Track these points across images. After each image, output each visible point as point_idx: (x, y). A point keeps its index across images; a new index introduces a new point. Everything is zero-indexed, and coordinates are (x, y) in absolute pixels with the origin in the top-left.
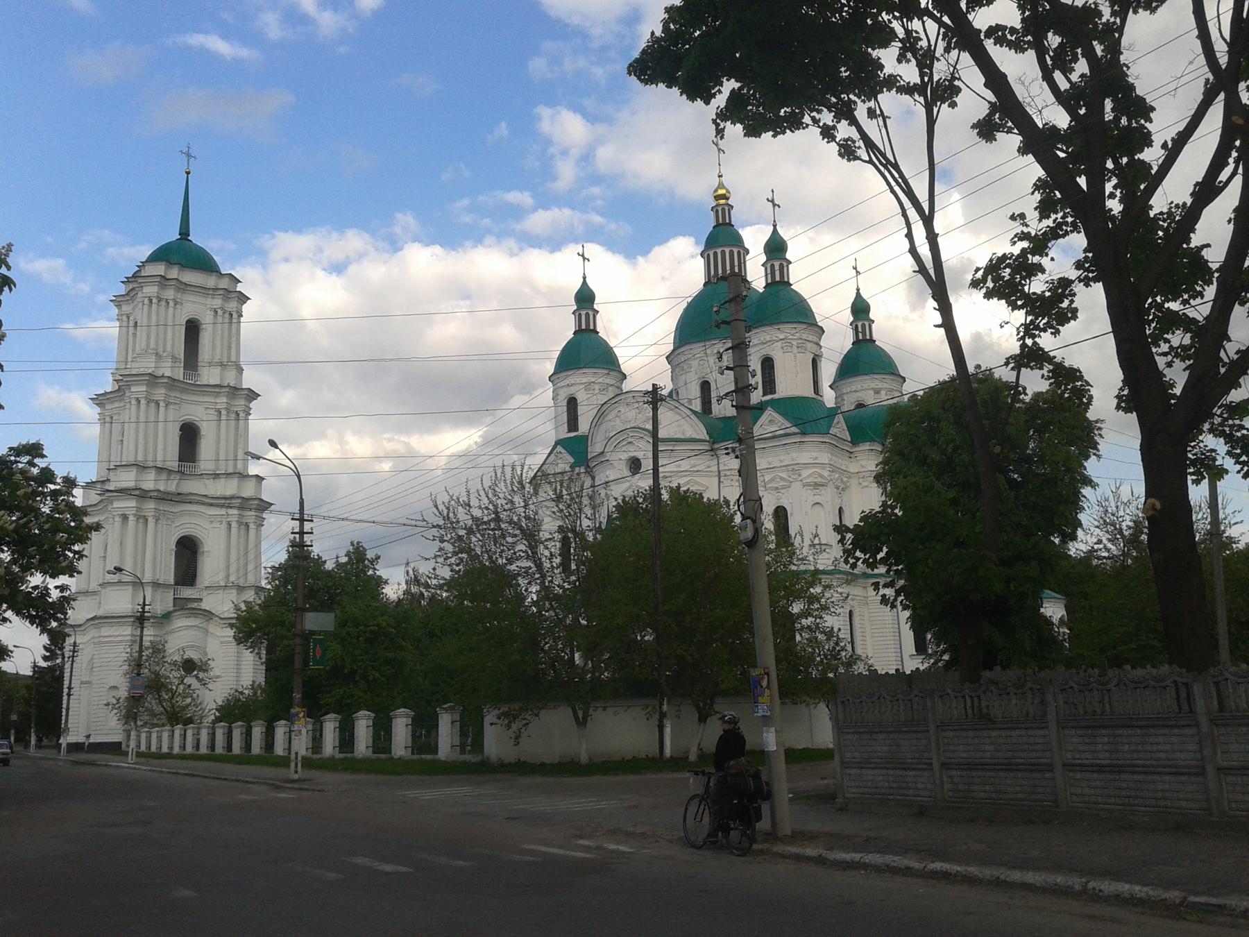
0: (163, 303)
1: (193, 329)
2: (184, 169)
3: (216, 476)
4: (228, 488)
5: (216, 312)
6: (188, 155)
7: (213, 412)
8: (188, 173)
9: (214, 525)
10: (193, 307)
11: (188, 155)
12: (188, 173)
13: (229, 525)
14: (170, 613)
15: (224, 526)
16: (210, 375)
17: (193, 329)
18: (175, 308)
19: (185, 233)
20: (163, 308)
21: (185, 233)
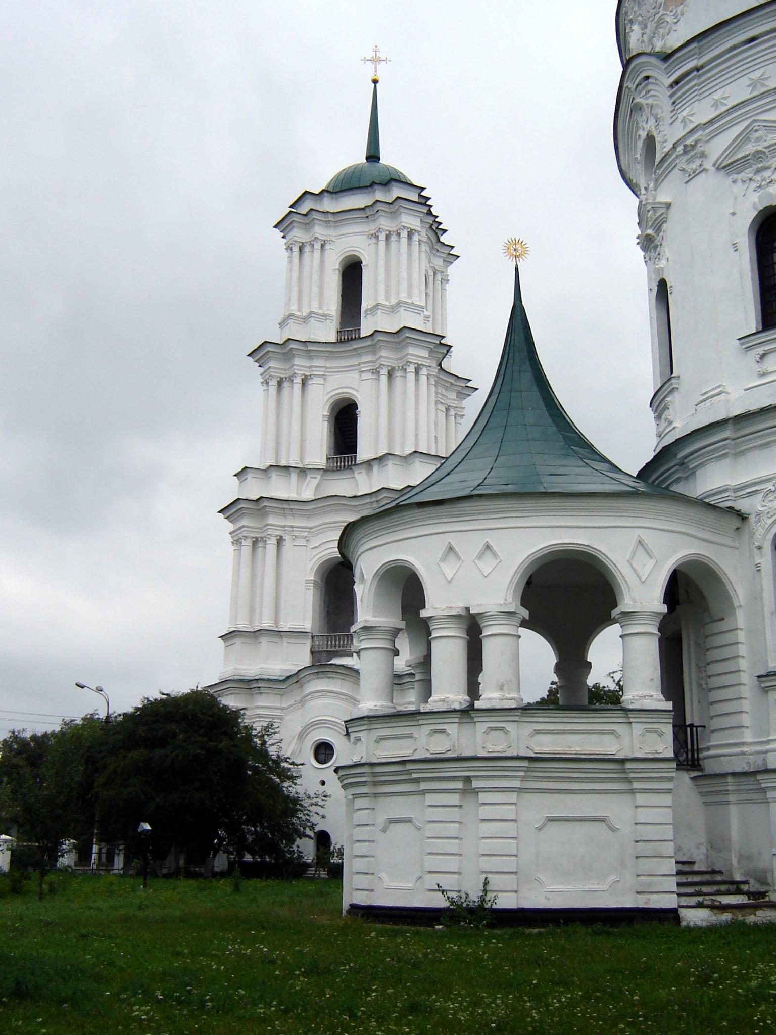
1: (352, 273)
8: (375, 82)
12: (375, 82)
17: (352, 273)
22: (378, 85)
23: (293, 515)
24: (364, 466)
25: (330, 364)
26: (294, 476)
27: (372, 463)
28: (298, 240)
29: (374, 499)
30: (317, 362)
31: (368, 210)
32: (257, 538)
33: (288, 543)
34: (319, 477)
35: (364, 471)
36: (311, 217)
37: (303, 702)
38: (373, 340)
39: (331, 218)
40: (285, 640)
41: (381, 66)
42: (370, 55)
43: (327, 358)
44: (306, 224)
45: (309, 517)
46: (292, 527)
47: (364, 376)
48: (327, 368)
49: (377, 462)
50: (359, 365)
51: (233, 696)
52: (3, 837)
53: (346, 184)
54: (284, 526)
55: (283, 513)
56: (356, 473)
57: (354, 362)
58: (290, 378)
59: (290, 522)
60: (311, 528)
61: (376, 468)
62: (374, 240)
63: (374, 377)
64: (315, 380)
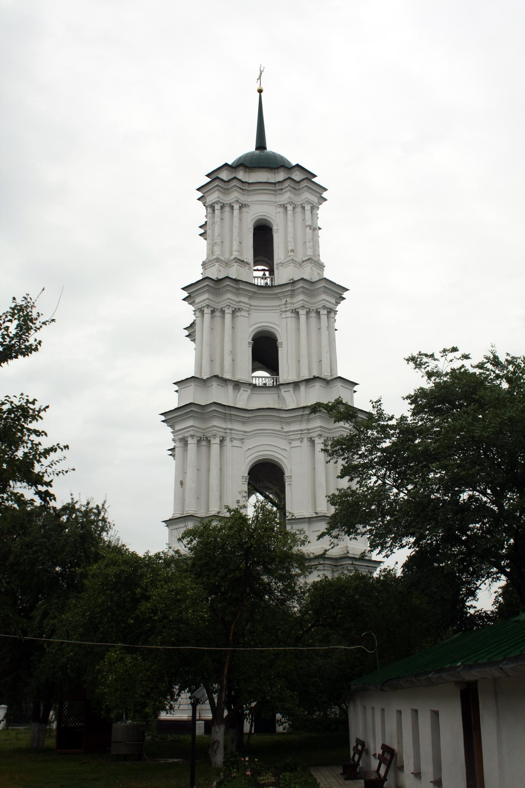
2: (257, 87)
8: (260, 91)
10: (262, 207)
12: (260, 91)
15: (306, 443)
19: (261, 144)
21: (261, 144)
22: (262, 94)
23: (231, 420)
24: (292, 386)
26: (230, 388)
28: (222, 201)
31: (277, 185)
33: (227, 443)
34: (249, 391)
35: (291, 390)
43: (250, 298)
44: (225, 189)
45: (244, 423)
46: (231, 429)
48: (250, 305)
49: (304, 383)
52: (3, 706)
53: (246, 164)
54: (225, 429)
56: (282, 391)
59: (229, 426)
61: (303, 388)
64: (243, 313)
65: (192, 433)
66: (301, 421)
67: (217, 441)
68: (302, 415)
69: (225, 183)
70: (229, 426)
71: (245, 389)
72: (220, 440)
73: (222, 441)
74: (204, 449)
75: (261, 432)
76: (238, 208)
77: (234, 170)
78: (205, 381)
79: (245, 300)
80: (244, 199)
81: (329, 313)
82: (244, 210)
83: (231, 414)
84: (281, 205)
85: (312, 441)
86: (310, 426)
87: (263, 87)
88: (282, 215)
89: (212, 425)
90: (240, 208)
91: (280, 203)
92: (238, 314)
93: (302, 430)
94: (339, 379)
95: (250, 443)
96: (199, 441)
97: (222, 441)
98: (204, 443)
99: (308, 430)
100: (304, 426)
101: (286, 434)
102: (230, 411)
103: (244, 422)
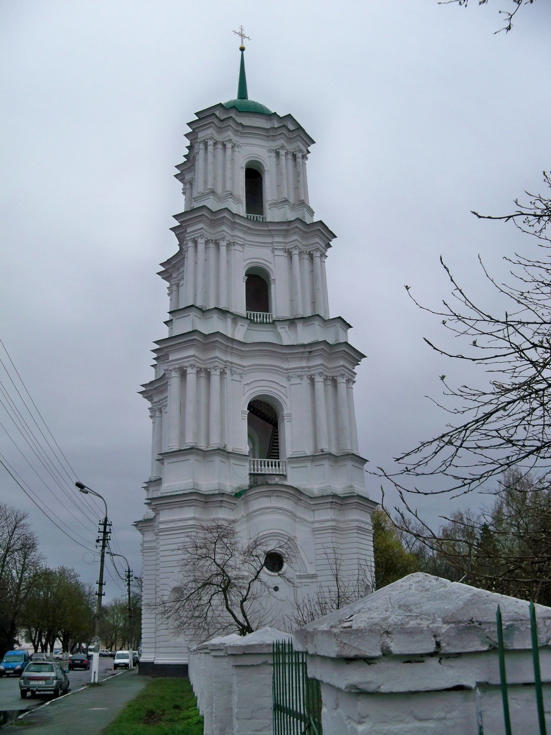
0: (220, 146)
2: (240, 45)
3: (292, 322)
4: (305, 335)
5: (278, 154)
6: (242, 36)
7: (281, 253)
8: (242, 49)
9: (295, 381)
11: (242, 36)
12: (242, 49)
13: (312, 380)
14: (245, 491)
16: (272, 214)
18: (233, 151)
20: (220, 151)
23: (232, 354)
25: (248, 238)
26: (229, 321)
27: (296, 321)
29: (308, 350)
30: (237, 233)
32: (201, 369)
33: (228, 376)
34: (246, 325)
36: (226, 124)
37: (249, 516)
38: (288, 226)
39: (240, 129)
40: (232, 461)
41: (245, 40)
42: (238, 31)
43: (245, 233)
45: (242, 357)
46: (232, 363)
47: (277, 253)
50: (272, 243)
51: (192, 508)
54: (226, 362)
55: (226, 350)
56: (278, 327)
57: (269, 240)
58: (216, 241)
60: (244, 367)
62: (273, 155)
63: (286, 255)
65: (192, 362)
66: (301, 358)
67: (218, 372)
68: (303, 352)
69: (214, 124)
70: (230, 360)
71: (242, 324)
72: (221, 372)
73: (223, 373)
74: (203, 381)
75: (262, 368)
76: (231, 147)
77: (226, 111)
78: (204, 311)
79: (240, 235)
80: (235, 139)
81: (321, 256)
82: (236, 149)
83: (232, 348)
84: (273, 150)
85: (312, 380)
86: (311, 364)
87: (245, 45)
88: (274, 159)
89: (214, 356)
90: (233, 147)
91: (272, 148)
92: (233, 248)
93: (302, 368)
94: (339, 319)
95: (248, 379)
96: (198, 372)
97: (223, 373)
98: (202, 375)
99: (309, 367)
100: (304, 364)
101: (286, 372)
102: (232, 344)
103: (243, 355)
